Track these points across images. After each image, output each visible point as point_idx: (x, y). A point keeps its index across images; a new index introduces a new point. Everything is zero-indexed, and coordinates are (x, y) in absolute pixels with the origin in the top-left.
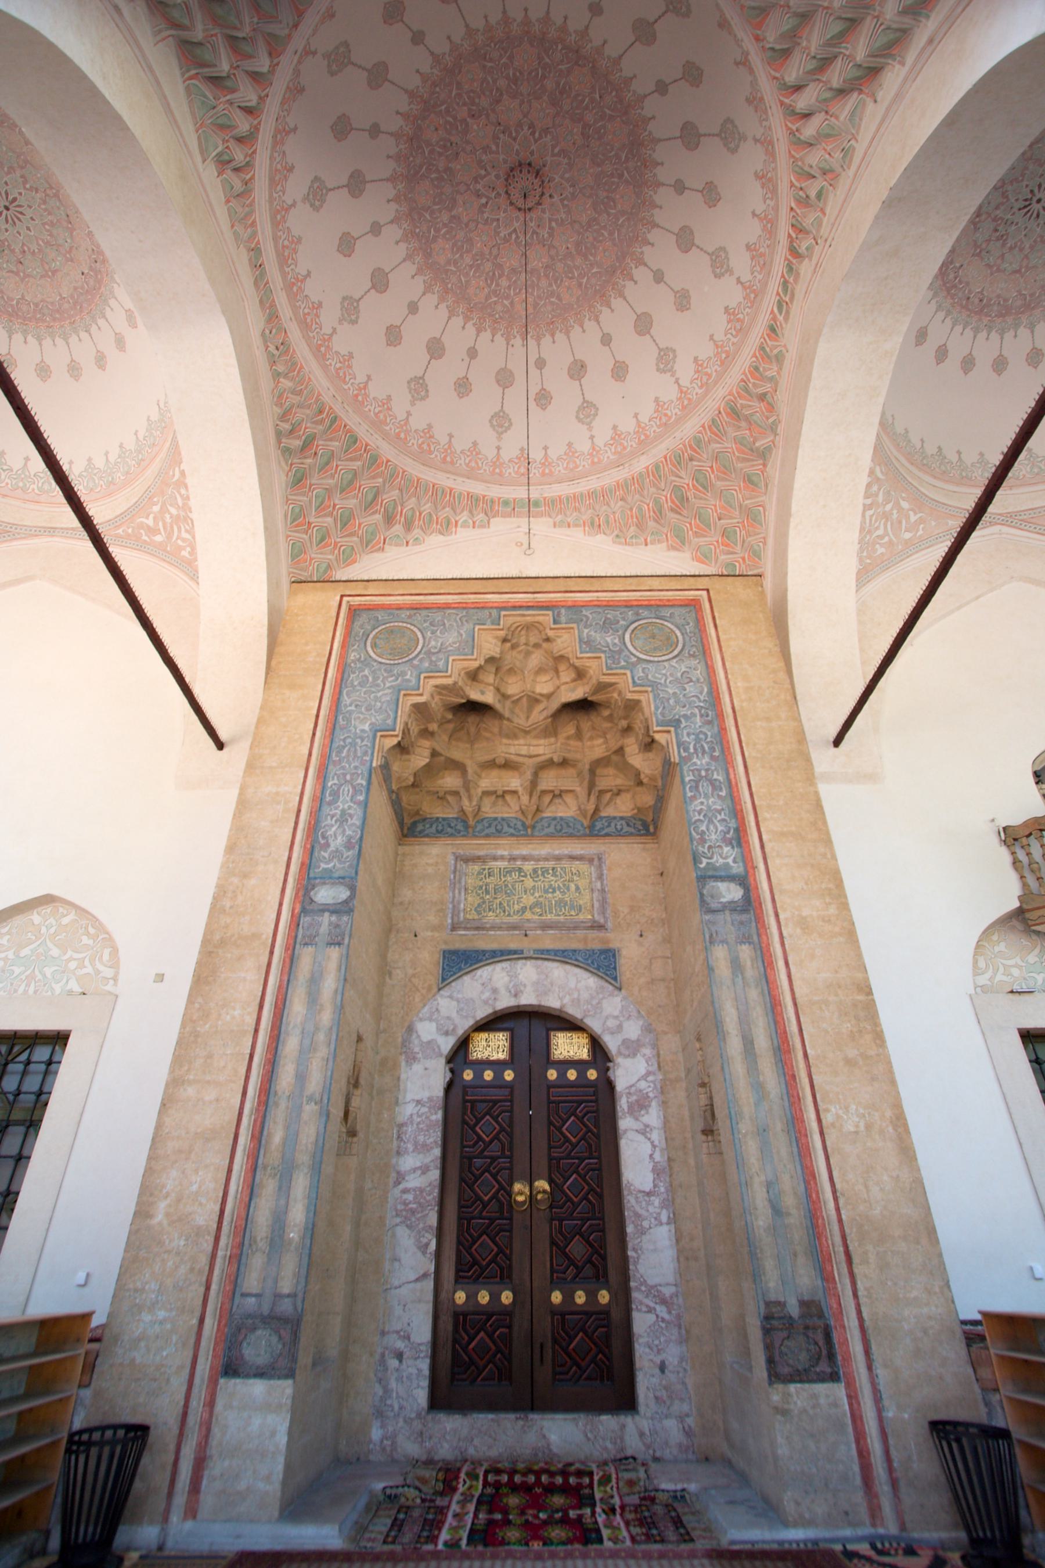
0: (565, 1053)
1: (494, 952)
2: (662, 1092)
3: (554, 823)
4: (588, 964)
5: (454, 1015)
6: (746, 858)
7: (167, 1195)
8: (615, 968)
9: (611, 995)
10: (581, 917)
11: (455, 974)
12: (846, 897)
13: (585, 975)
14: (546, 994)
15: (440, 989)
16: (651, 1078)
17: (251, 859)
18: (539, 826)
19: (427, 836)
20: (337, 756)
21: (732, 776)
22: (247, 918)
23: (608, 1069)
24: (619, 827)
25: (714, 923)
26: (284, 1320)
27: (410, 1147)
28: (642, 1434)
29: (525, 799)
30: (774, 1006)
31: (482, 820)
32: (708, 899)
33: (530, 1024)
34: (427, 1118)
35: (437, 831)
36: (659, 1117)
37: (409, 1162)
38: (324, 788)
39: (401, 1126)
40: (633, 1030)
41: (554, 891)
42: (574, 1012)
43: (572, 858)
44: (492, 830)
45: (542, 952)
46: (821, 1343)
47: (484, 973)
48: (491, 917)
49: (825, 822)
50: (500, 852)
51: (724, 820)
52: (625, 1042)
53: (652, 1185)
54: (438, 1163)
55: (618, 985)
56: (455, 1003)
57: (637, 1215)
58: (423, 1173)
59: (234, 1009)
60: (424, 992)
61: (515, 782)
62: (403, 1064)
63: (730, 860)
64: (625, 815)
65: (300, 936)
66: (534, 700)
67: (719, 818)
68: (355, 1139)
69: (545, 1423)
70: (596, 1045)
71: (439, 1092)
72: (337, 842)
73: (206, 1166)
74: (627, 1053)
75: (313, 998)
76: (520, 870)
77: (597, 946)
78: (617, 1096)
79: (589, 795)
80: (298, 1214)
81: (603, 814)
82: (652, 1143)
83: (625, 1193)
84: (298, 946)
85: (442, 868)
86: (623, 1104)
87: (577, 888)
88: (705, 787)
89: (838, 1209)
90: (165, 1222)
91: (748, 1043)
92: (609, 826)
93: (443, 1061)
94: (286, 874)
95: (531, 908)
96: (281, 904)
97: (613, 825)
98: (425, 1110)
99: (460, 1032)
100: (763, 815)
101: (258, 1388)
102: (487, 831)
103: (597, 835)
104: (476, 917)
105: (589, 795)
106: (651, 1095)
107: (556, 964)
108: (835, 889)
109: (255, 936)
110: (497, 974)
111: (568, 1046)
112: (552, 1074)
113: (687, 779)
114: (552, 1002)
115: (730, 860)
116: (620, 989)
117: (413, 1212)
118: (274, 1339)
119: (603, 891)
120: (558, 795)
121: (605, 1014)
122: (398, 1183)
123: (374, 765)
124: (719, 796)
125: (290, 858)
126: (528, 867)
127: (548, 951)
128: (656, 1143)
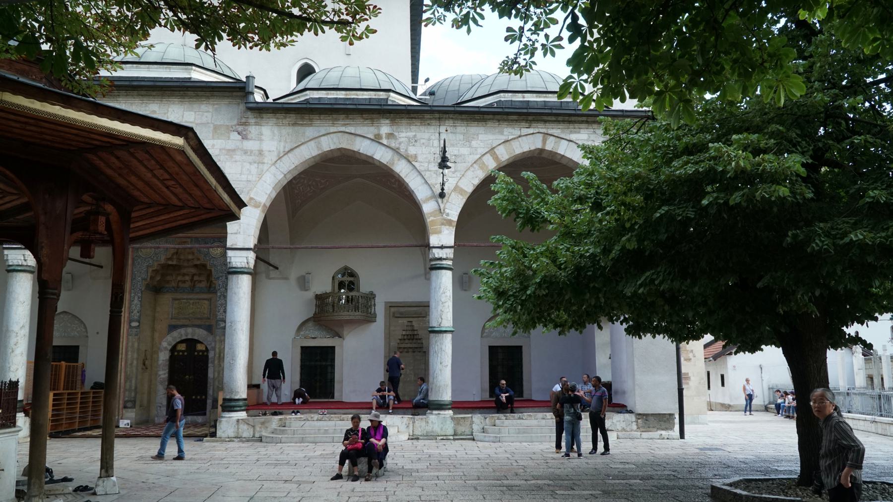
33: (191, 343)
37: (161, 373)
61: (187, 278)
66: (188, 260)
111: (200, 347)
120: (200, 281)
126: (191, 302)
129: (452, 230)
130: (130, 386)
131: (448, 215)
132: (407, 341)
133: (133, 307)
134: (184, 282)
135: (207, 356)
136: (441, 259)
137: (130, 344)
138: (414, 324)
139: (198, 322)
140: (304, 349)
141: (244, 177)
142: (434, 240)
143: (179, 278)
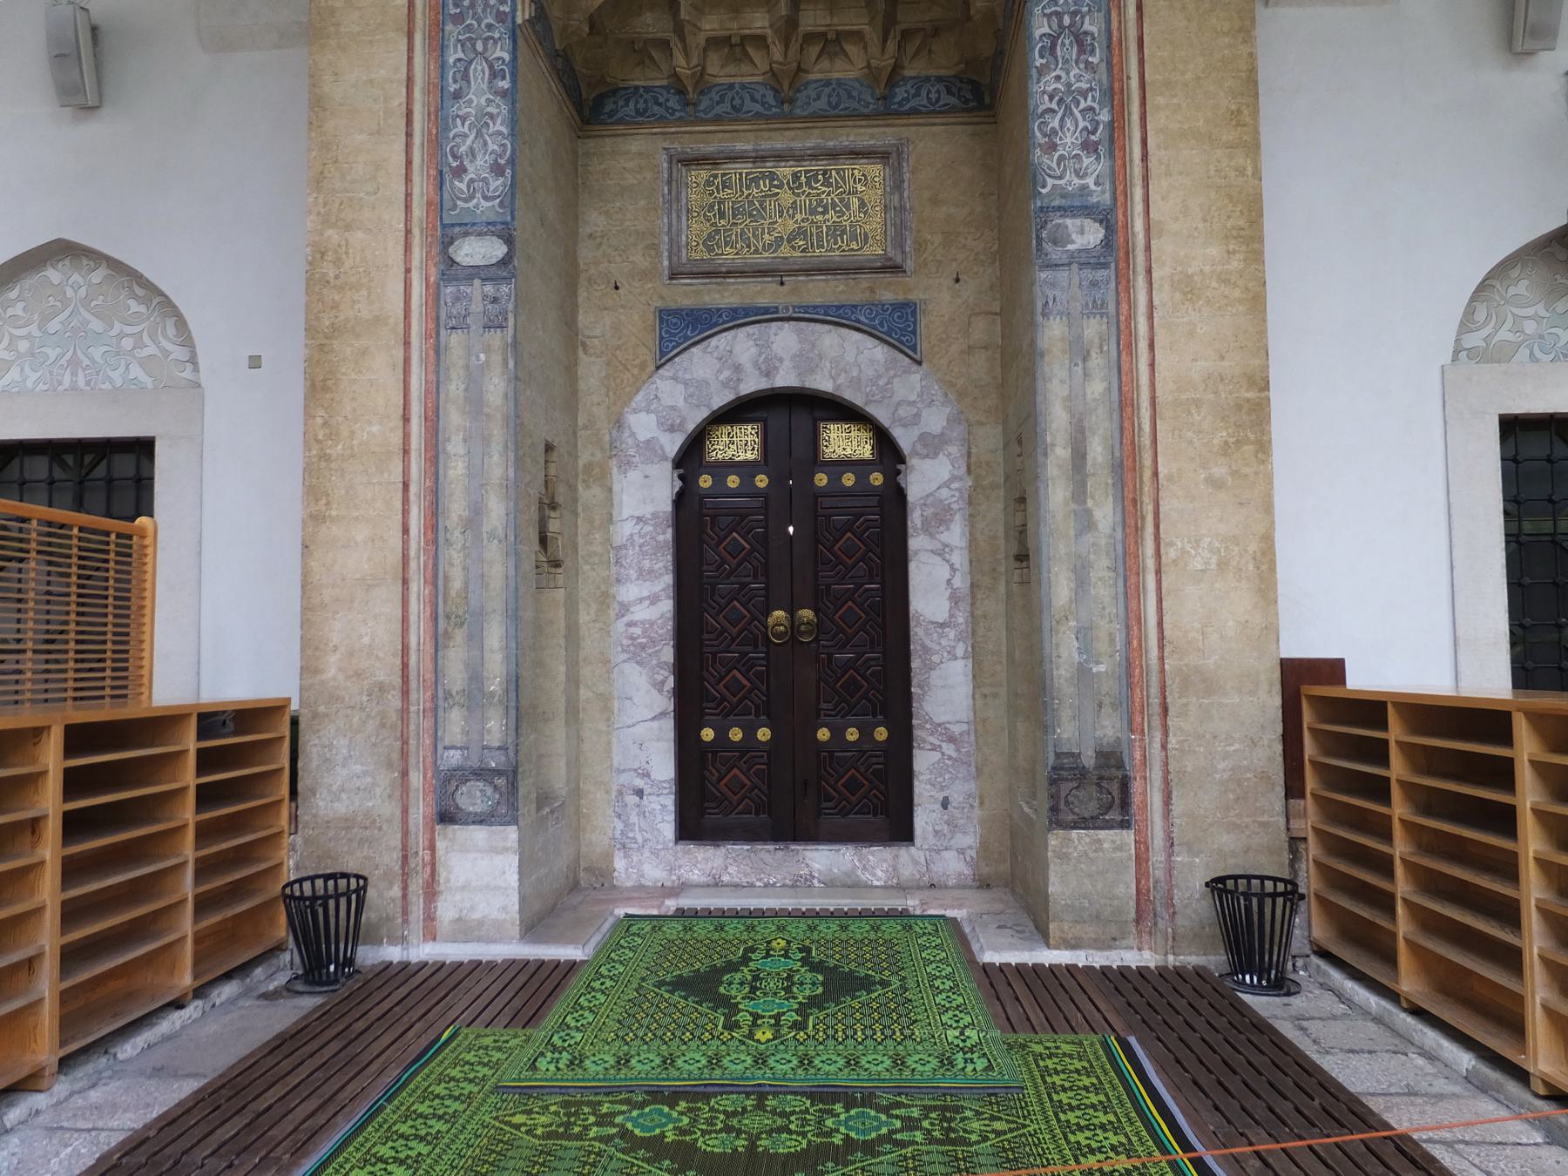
0: (840, 451)
1: (735, 310)
2: (970, 503)
3: (827, 90)
4: (874, 328)
5: (681, 403)
6: (1118, 179)
7: (335, 648)
8: (914, 332)
9: (907, 372)
10: (867, 251)
11: (679, 345)
12: (1261, 240)
13: (870, 342)
14: (812, 371)
15: (658, 368)
16: (955, 485)
17: (351, 199)
18: (801, 97)
19: (620, 122)
20: (456, 5)
21: (1115, 25)
22: (364, 292)
23: (899, 472)
24: (933, 96)
25: (1053, 285)
26: (498, 773)
27: (633, 573)
28: (916, 863)
29: (777, 53)
30: (1125, 405)
31: (710, 89)
32: (1048, 247)
33: (791, 412)
34: (653, 538)
35: (637, 111)
36: (963, 534)
37: (629, 592)
38: (443, 66)
39: (620, 548)
40: (935, 420)
41: (825, 212)
42: (855, 397)
43: (856, 154)
44: (725, 107)
45: (806, 309)
46: (1116, 793)
47: (721, 342)
48: (728, 256)
49: (1255, 113)
50: (740, 146)
51: (1091, 109)
52: (922, 437)
53: (946, 615)
54: (670, 592)
55: (917, 357)
56: (681, 387)
57: (926, 650)
58: (652, 603)
59: (370, 423)
60: (636, 371)
62: (615, 470)
63: (1090, 181)
64: (943, 72)
65: (443, 316)
67: (1083, 105)
68: (559, 570)
69: (808, 854)
70: (883, 439)
71: (667, 507)
72: (478, 167)
73: (375, 617)
74: (925, 452)
75: (475, 403)
76: (772, 176)
77: (887, 296)
78: (910, 506)
79: (885, 41)
81: (908, 73)
82: (952, 566)
83: (912, 624)
84: (443, 332)
85: (649, 175)
86: (915, 518)
87: (862, 204)
88: (1067, 49)
89: (1162, 659)
90: (341, 677)
91: (1079, 456)
92: (917, 94)
93: (669, 466)
94: (408, 220)
95: (789, 241)
96: (408, 271)
97: (924, 92)
98: (648, 528)
99: (691, 427)
100: (1154, 100)
101: (479, 834)
102: (719, 110)
103: (898, 114)
104: (706, 256)
105: (885, 41)
106: (955, 506)
107: (827, 327)
108: (1247, 230)
109: (379, 320)
110: (741, 344)
111: (843, 442)
112: (821, 480)
113: (1037, 33)
114: (823, 383)
115: (1090, 181)
116: (919, 363)
117: (643, 647)
118: (489, 791)
119: (902, 208)
120: (831, 44)
121: (896, 399)
122: (620, 615)
123: (519, 21)
124: (1087, 63)
125: (408, 196)
126: (785, 171)
127: (815, 307)
128: (957, 566)
130: (476, 676)
133: (463, 136)
134: (735, 47)
135: (896, 498)
137: (455, 387)
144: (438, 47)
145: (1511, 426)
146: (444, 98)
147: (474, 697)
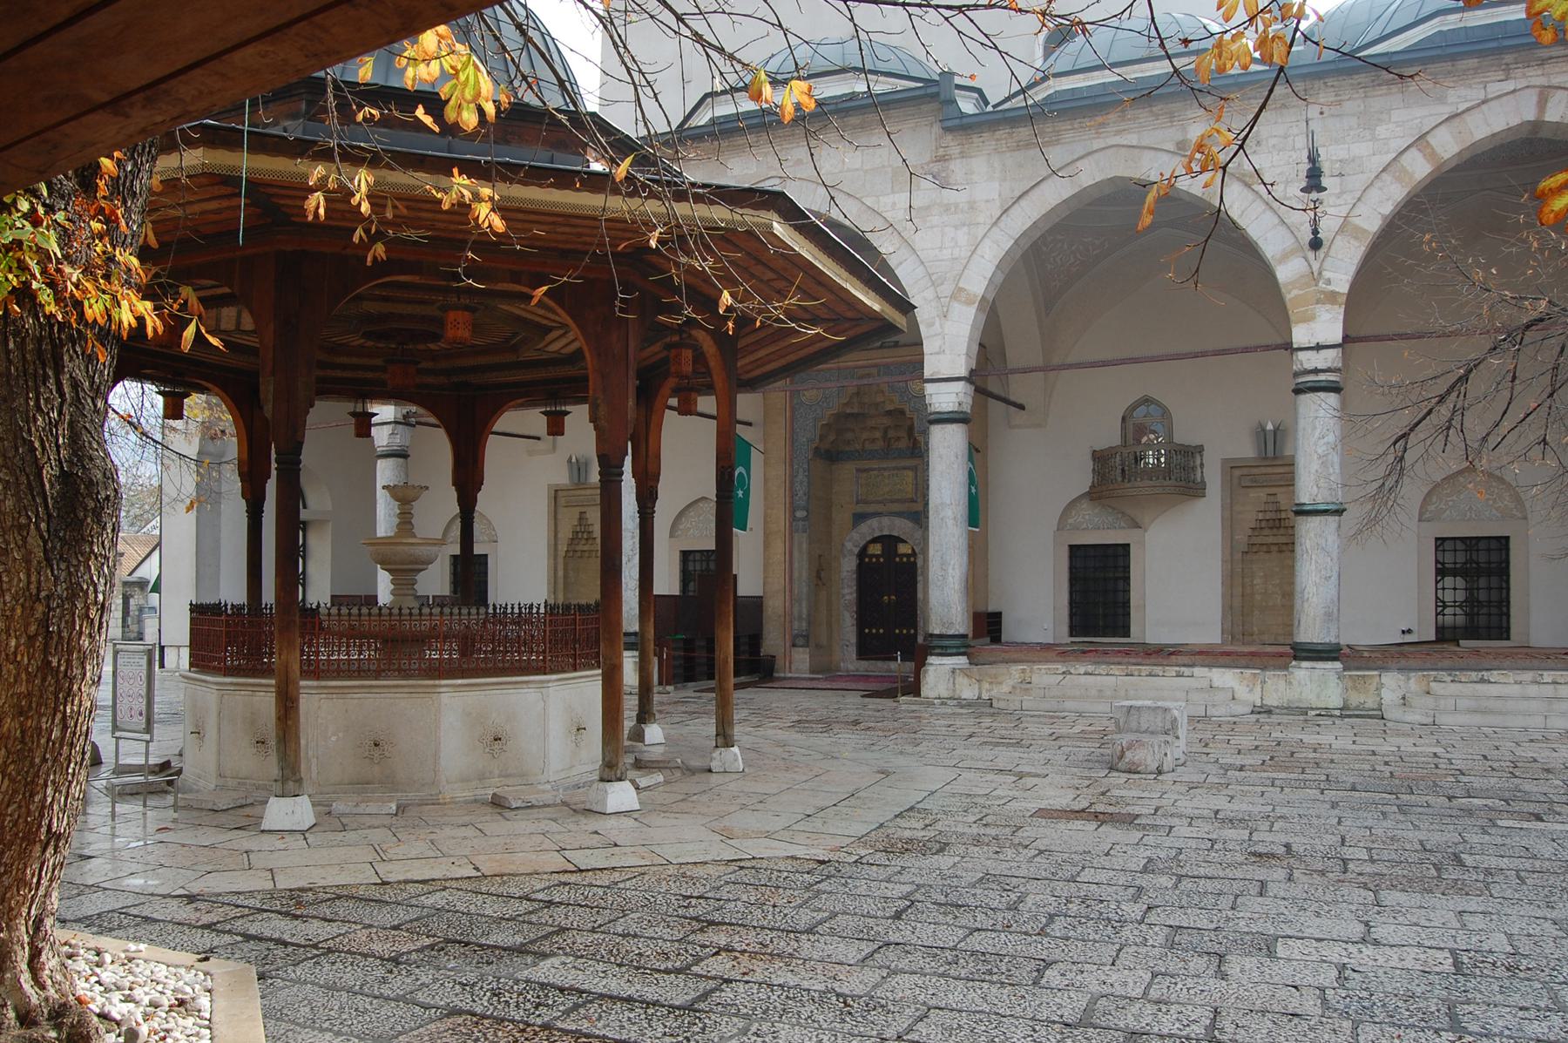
33: (889, 542)
37: (846, 591)
80: (805, 611)
110: (874, 522)
111: (903, 549)
120: (898, 439)
129: (1338, 313)
131: (1329, 282)
132: (1266, 532)
134: (874, 441)
135: (915, 563)
136: (1316, 371)
138: (1280, 498)
139: (896, 507)
140: (1074, 550)
141: (947, 253)
142: (1300, 335)
143: (865, 435)
144: (792, 466)
145: (1074, 550)
146: (793, 477)
147: (800, 618)
